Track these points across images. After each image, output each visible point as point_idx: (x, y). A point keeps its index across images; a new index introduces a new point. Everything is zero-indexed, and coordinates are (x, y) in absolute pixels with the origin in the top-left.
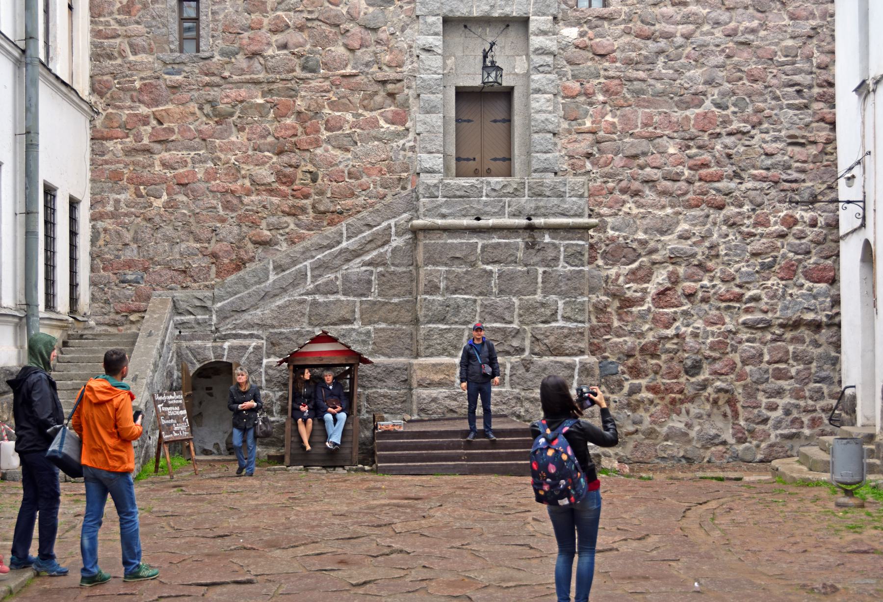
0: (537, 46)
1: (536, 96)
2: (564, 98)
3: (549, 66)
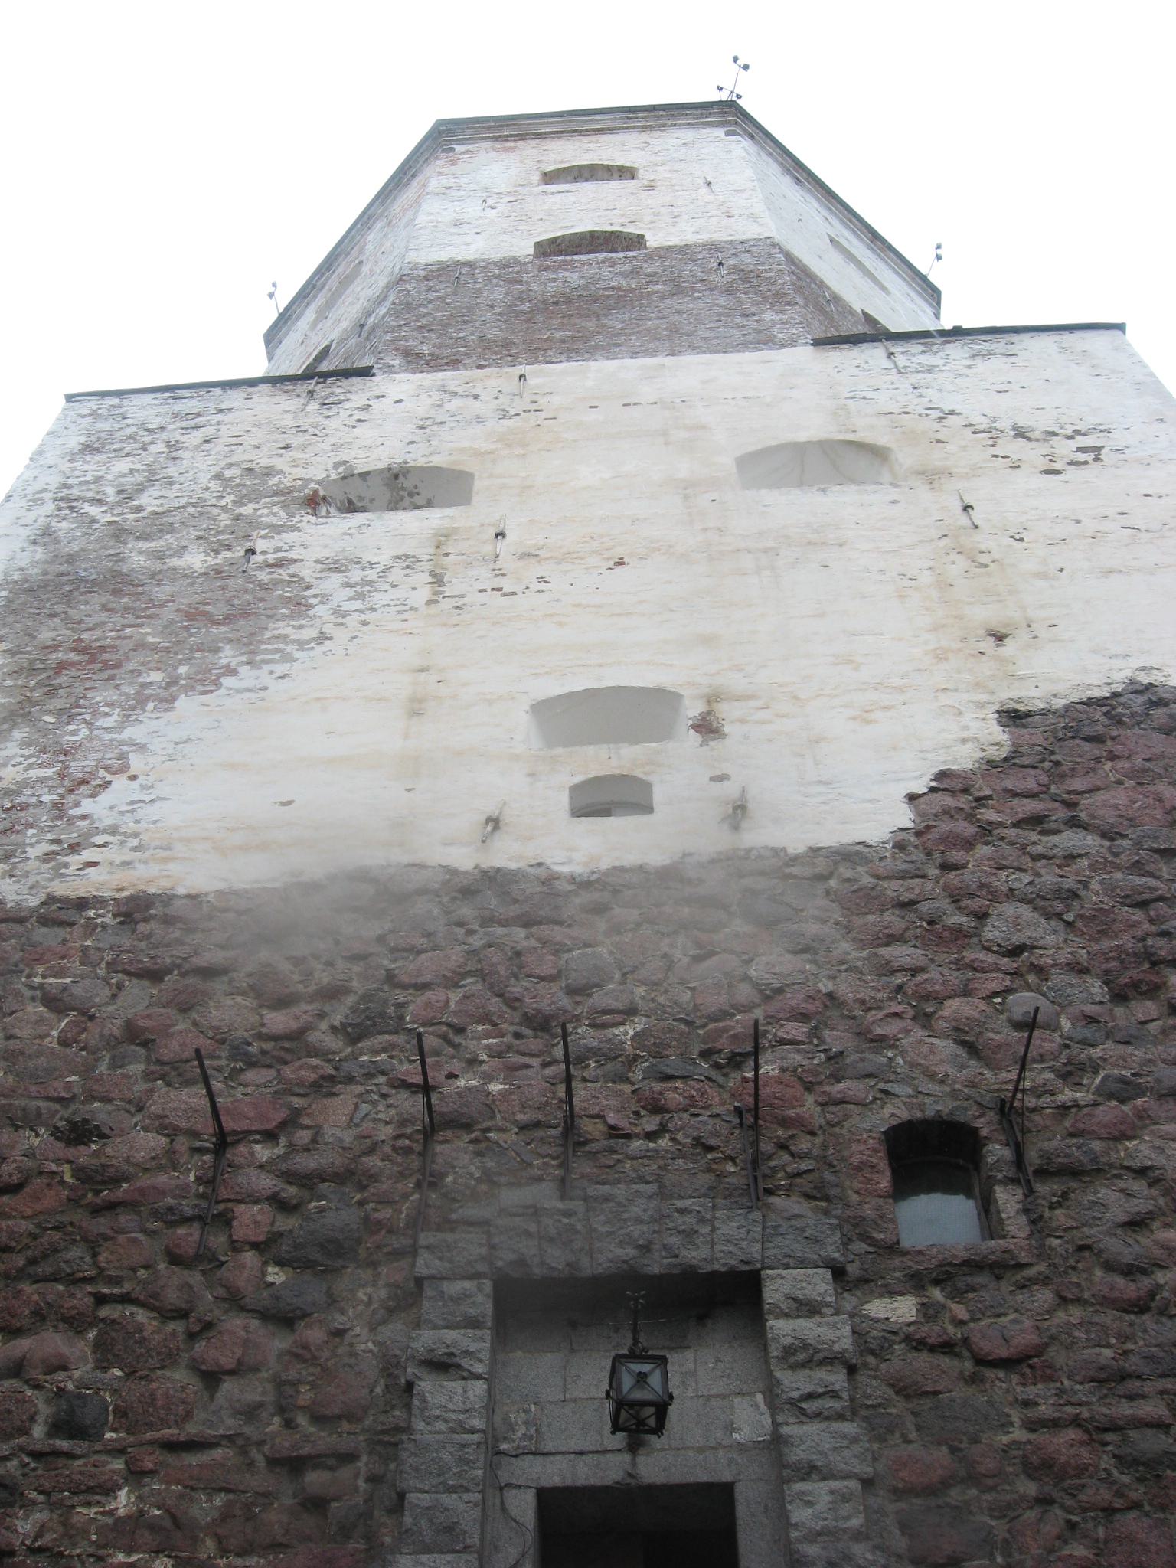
0: (788, 1341)
1: (799, 1486)
2: (898, 1494)
3: (834, 1395)
